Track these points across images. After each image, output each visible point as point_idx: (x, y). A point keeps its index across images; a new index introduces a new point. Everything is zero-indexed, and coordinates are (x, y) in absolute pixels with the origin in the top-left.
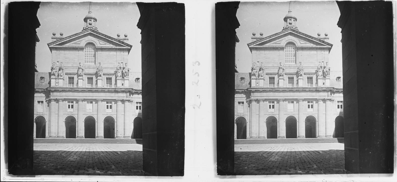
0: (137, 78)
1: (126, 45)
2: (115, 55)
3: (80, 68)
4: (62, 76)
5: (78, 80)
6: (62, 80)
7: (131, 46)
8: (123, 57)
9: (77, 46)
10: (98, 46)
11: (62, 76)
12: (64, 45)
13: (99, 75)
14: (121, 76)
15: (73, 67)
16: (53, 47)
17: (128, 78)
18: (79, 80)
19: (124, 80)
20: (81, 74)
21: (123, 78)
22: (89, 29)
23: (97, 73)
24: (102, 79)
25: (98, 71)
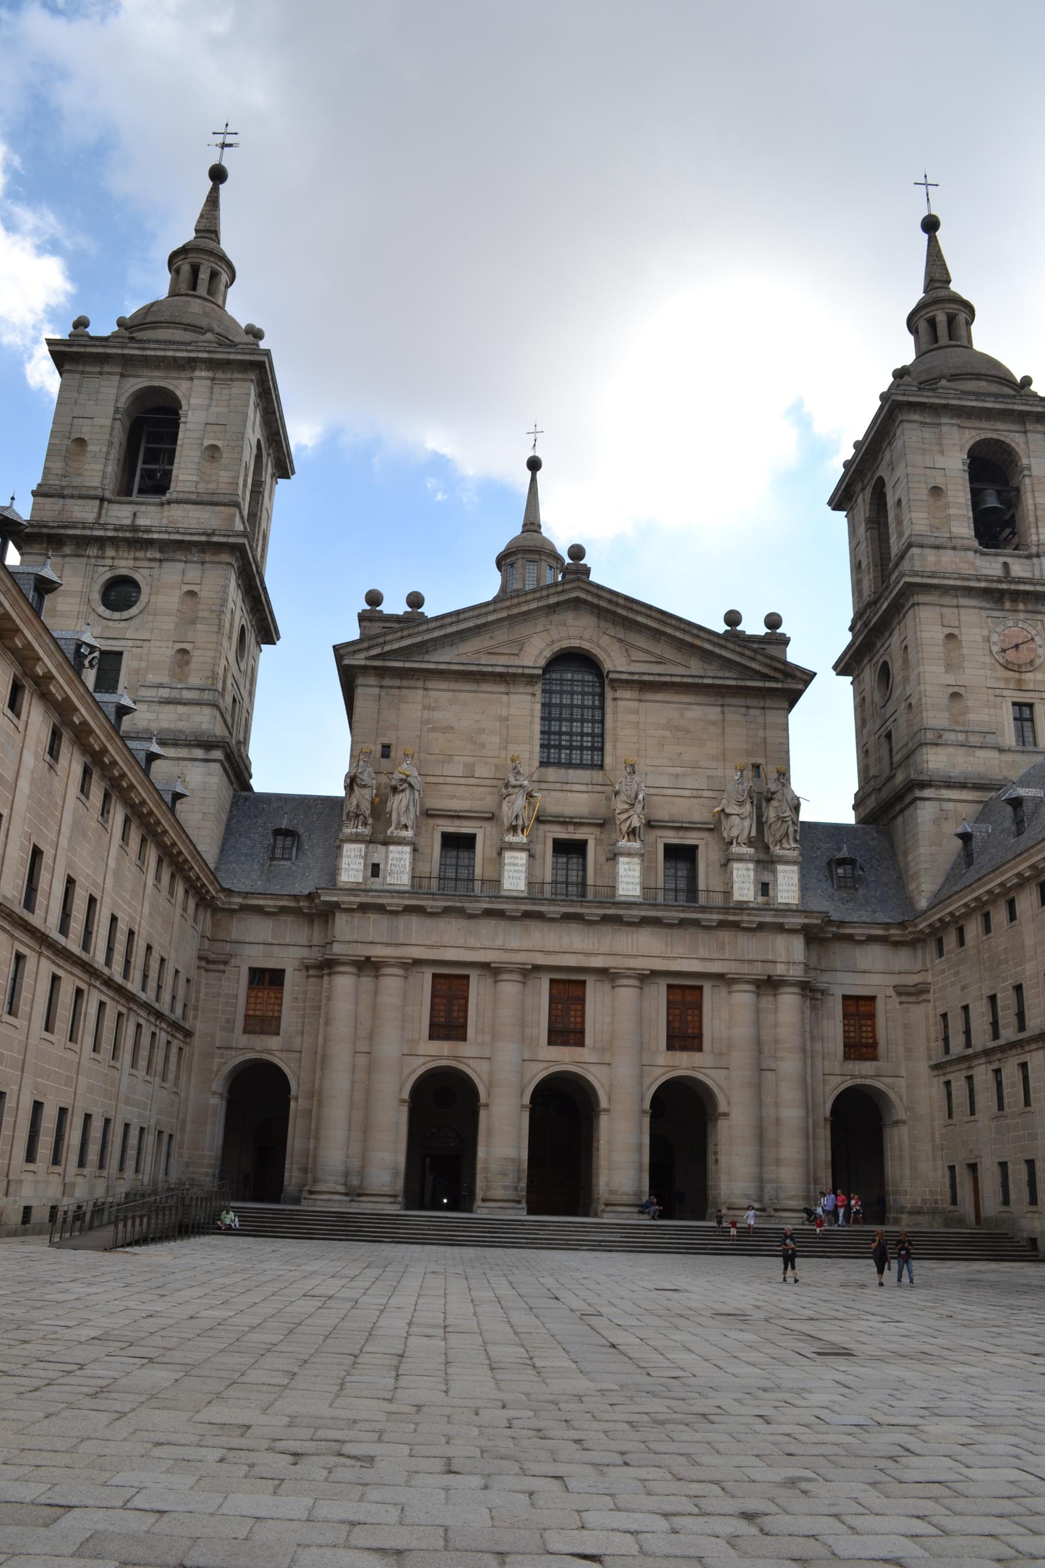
1: (776, 669)
2: (714, 723)
3: (514, 787)
5: (500, 854)
6: (408, 849)
7: (805, 677)
9: (500, 663)
10: (619, 669)
11: (406, 827)
12: (427, 658)
13: (624, 828)
15: (472, 781)
16: (363, 663)
17: (796, 853)
19: (773, 862)
20: (520, 822)
22: (573, 581)
23: (614, 818)
24: (642, 855)
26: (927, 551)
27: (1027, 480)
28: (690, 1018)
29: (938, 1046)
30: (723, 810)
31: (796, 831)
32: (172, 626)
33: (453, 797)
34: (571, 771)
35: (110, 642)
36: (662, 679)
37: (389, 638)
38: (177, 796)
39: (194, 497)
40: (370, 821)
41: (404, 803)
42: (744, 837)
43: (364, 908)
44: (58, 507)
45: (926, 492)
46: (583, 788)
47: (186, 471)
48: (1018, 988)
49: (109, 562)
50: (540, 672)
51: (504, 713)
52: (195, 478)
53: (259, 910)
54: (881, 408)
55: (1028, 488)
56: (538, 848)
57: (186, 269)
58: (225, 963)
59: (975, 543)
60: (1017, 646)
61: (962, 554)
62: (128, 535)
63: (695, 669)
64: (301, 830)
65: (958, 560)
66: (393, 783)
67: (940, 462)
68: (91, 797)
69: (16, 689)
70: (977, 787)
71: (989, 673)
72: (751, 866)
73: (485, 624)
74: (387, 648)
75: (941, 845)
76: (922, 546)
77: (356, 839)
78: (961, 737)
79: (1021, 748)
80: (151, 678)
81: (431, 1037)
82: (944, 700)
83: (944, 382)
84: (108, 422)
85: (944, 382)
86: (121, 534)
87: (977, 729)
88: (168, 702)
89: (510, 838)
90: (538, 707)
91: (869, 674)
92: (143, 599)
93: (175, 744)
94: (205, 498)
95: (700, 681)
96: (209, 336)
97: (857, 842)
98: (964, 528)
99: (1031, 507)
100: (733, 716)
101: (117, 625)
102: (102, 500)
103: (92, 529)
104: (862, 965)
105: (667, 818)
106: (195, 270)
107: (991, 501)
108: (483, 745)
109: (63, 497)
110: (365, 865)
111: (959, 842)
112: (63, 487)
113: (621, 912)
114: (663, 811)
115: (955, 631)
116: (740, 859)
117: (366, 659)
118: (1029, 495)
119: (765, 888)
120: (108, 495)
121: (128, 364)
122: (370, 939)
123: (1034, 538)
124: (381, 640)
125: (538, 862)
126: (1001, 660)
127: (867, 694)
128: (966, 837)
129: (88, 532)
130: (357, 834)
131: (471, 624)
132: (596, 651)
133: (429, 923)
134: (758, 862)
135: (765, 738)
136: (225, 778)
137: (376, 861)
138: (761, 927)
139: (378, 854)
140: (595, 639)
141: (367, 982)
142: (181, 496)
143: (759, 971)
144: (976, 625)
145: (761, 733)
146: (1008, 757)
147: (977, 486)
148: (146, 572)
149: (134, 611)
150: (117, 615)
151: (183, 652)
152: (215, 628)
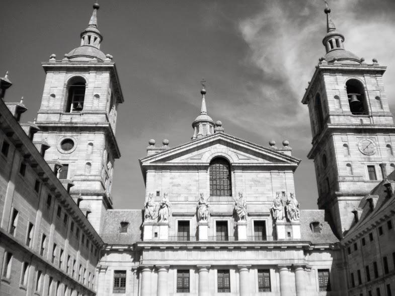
0: (312, 221)
2: (268, 179)
4: (166, 219)
5: (198, 228)
8: (284, 181)
9: (195, 162)
10: (235, 162)
11: (166, 219)
12: (170, 161)
14: (283, 218)
15: (187, 202)
16: (149, 164)
18: (200, 227)
19: (291, 225)
21: (288, 220)
25: (239, 209)
26: (335, 117)
27: (366, 92)
28: (266, 281)
29: (350, 284)
30: (273, 208)
31: (298, 214)
32: (85, 155)
33: (181, 208)
34: (221, 198)
35: (64, 161)
36: (250, 165)
37: (157, 156)
38: (88, 212)
39: (91, 112)
40: (153, 218)
41: (165, 211)
42: (280, 217)
43: (153, 249)
44: (46, 117)
45: (333, 97)
46: (225, 203)
47: (89, 102)
48: (375, 264)
49: (63, 134)
50: (209, 164)
51: (197, 179)
52: (91, 105)
53: (116, 251)
54: (316, 71)
55: (366, 94)
56: (211, 224)
57: (86, 37)
58: (106, 269)
59: (351, 113)
60: (367, 147)
61: (347, 117)
62: (69, 125)
63: (261, 161)
64: (130, 222)
65: (345, 119)
66: (161, 205)
67: (337, 87)
68: (61, 216)
69: (37, 183)
70: (358, 195)
71: (358, 156)
72: (284, 226)
73: (189, 150)
74: (157, 159)
75: (347, 216)
76: (333, 115)
77: (149, 224)
78: (351, 178)
79: (371, 181)
80: (79, 173)
81: (177, 292)
82: (345, 166)
83: (336, 61)
84: (62, 88)
85: (336, 61)
86: (67, 125)
87: (356, 175)
88: (84, 180)
89: (202, 221)
90: (208, 177)
91: (319, 158)
92: (75, 146)
93: (87, 195)
94: (95, 112)
95: (261, 165)
96: (95, 59)
97: (319, 216)
98: (347, 109)
99: (368, 100)
100: (275, 174)
101: (66, 155)
102: (60, 114)
103: (57, 124)
104: (324, 259)
105: (254, 212)
106: (89, 37)
107: (355, 99)
108: (190, 190)
109: (48, 113)
110: (153, 233)
111: (353, 214)
112: (48, 110)
113: (240, 245)
114: (253, 209)
115: (346, 143)
116: (280, 225)
117: (150, 163)
118: (367, 97)
119: (289, 233)
120: (62, 112)
121: (68, 70)
122: (155, 259)
123: (370, 110)
124: (155, 156)
125: (211, 229)
126: (362, 152)
127: (319, 165)
128: (355, 212)
129: (56, 125)
130: (149, 223)
131: (185, 150)
132: (227, 156)
133: (175, 253)
134: (286, 225)
135: (286, 183)
136: (104, 207)
137: (156, 232)
138: (289, 248)
139: (157, 229)
140: (226, 152)
141: (154, 275)
142: (86, 112)
143: (289, 263)
144: (352, 139)
145: (284, 181)
146: (366, 184)
147: (350, 94)
148: (75, 137)
149: (72, 150)
150: (66, 152)
151: (89, 164)
152: (99, 155)
